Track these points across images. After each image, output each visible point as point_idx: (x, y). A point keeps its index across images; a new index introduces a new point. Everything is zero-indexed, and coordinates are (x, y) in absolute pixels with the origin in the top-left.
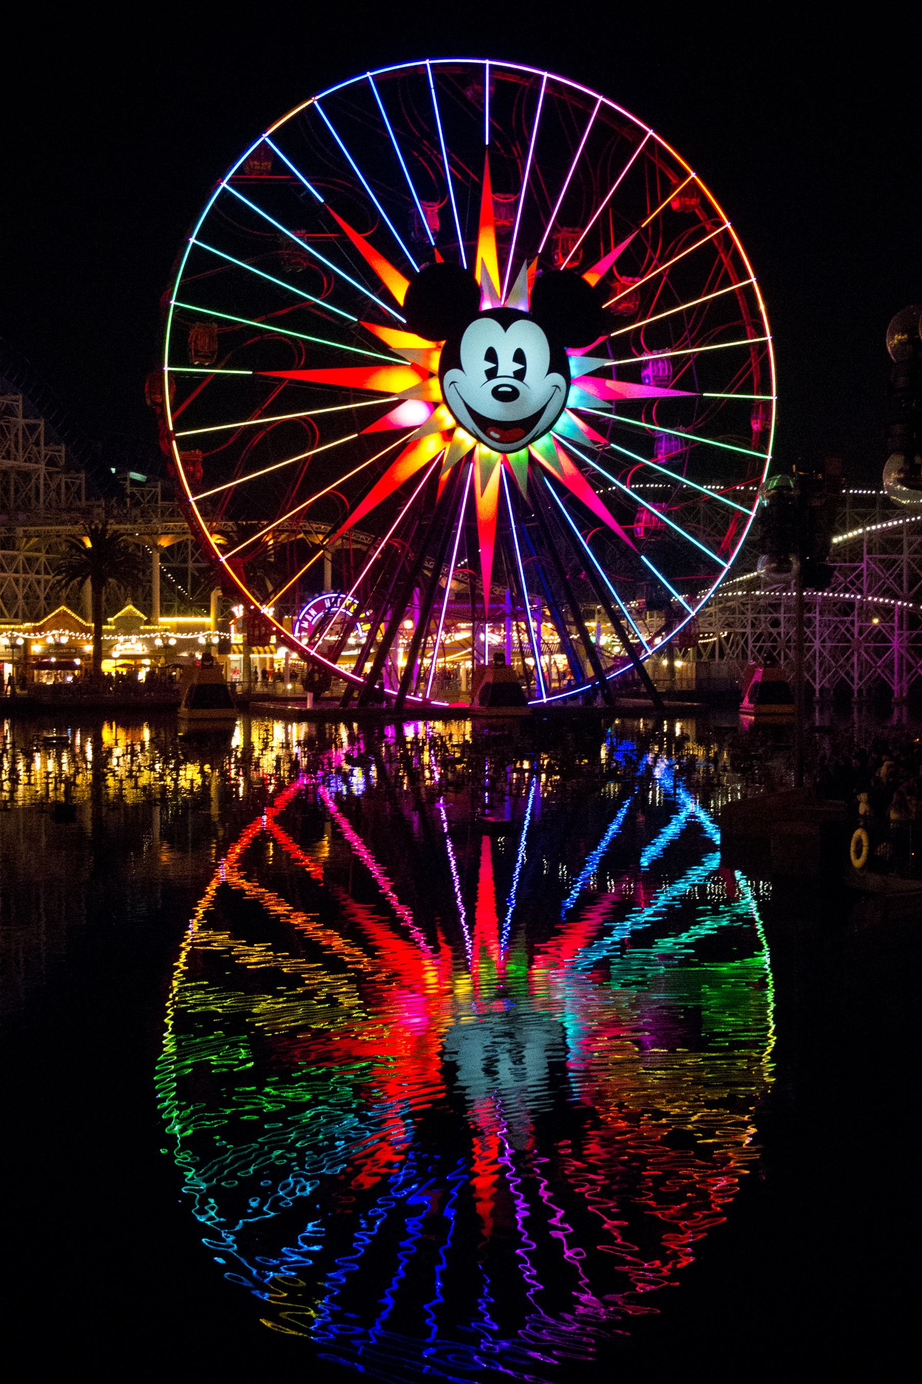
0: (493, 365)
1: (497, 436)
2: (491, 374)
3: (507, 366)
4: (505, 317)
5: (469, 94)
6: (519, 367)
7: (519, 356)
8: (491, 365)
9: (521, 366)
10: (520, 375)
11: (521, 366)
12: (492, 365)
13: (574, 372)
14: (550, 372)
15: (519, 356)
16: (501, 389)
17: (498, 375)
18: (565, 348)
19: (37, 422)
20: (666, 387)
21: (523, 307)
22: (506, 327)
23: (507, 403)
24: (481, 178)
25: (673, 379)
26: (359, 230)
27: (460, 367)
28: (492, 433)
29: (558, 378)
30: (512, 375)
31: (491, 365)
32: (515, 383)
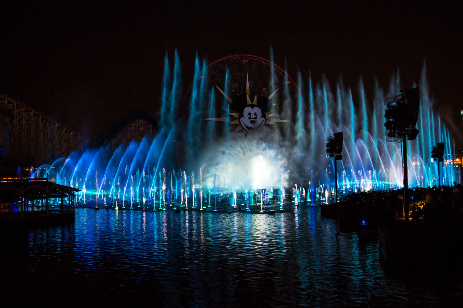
0: (250, 116)
1: (251, 131)
2: (250, 118)
3: (253, 116)
4: (252, 106)
5: (243, 62)
6: (255, 116)
7: (255, 114)
8: (249, 116)
9: (255, 116)
10: (256, 118)
12: (250, 116)
13: (267, 117)
14: (261, 117)
15: (255, 114)
18: (265, 113)
19: (155, 130)
21: (256, 104)
22: (252, 109)
23: (252, 124)
24: (246, 78)
27: (244, 117)
28: (251, 130)
29: (263, 119)
30: (254, 118)
31: (249, 116)
32: (254, 120)
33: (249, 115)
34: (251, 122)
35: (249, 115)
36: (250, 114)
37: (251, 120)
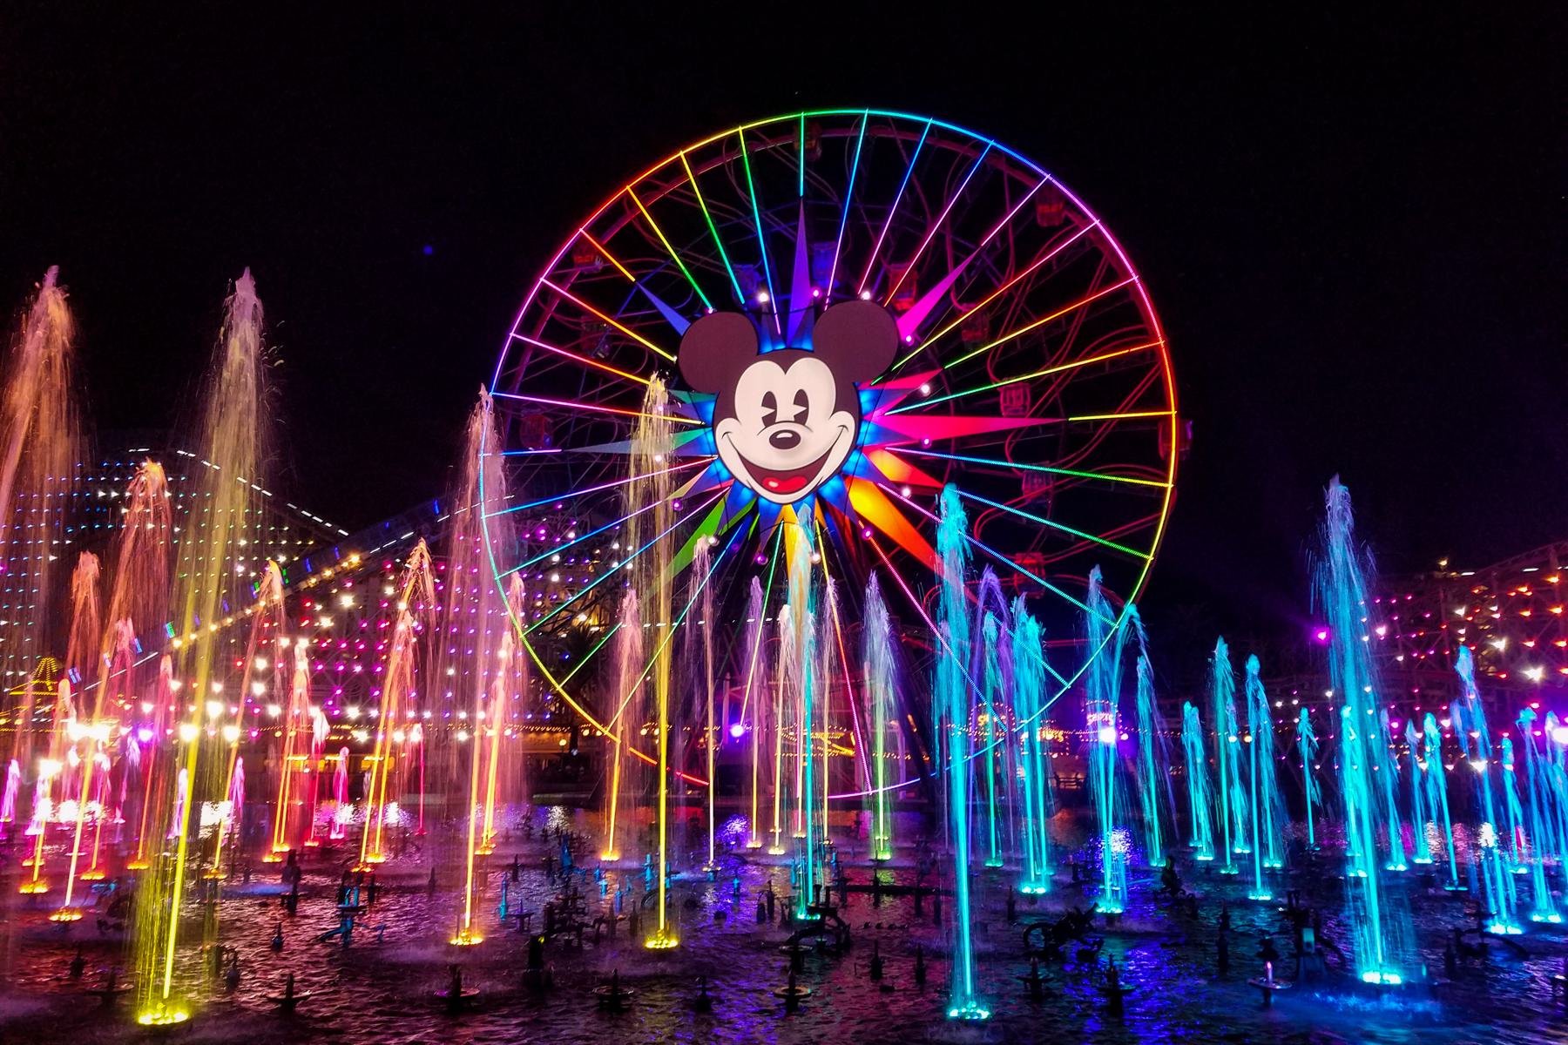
0: (772, 411)
2: (769, 420)
3: (787, 409)
7: (801, 399)
10: (801, 419)
11: (804, 409)
12: (772, 411)
15: (801, 399)
16: (779, 436)
17: (777, 420)
20: (1023, 416)
22: (785, 369)
25: (1032, 406)
26: (671, 303)
28: (773, 484)
29: (846, 418)
32: (797, 428)
33: (764, 404)
34: (776, 442)
35: (764, 404)
36: (769, 400)
37: (773, 429)
